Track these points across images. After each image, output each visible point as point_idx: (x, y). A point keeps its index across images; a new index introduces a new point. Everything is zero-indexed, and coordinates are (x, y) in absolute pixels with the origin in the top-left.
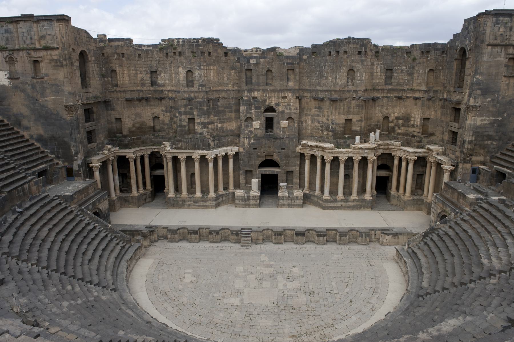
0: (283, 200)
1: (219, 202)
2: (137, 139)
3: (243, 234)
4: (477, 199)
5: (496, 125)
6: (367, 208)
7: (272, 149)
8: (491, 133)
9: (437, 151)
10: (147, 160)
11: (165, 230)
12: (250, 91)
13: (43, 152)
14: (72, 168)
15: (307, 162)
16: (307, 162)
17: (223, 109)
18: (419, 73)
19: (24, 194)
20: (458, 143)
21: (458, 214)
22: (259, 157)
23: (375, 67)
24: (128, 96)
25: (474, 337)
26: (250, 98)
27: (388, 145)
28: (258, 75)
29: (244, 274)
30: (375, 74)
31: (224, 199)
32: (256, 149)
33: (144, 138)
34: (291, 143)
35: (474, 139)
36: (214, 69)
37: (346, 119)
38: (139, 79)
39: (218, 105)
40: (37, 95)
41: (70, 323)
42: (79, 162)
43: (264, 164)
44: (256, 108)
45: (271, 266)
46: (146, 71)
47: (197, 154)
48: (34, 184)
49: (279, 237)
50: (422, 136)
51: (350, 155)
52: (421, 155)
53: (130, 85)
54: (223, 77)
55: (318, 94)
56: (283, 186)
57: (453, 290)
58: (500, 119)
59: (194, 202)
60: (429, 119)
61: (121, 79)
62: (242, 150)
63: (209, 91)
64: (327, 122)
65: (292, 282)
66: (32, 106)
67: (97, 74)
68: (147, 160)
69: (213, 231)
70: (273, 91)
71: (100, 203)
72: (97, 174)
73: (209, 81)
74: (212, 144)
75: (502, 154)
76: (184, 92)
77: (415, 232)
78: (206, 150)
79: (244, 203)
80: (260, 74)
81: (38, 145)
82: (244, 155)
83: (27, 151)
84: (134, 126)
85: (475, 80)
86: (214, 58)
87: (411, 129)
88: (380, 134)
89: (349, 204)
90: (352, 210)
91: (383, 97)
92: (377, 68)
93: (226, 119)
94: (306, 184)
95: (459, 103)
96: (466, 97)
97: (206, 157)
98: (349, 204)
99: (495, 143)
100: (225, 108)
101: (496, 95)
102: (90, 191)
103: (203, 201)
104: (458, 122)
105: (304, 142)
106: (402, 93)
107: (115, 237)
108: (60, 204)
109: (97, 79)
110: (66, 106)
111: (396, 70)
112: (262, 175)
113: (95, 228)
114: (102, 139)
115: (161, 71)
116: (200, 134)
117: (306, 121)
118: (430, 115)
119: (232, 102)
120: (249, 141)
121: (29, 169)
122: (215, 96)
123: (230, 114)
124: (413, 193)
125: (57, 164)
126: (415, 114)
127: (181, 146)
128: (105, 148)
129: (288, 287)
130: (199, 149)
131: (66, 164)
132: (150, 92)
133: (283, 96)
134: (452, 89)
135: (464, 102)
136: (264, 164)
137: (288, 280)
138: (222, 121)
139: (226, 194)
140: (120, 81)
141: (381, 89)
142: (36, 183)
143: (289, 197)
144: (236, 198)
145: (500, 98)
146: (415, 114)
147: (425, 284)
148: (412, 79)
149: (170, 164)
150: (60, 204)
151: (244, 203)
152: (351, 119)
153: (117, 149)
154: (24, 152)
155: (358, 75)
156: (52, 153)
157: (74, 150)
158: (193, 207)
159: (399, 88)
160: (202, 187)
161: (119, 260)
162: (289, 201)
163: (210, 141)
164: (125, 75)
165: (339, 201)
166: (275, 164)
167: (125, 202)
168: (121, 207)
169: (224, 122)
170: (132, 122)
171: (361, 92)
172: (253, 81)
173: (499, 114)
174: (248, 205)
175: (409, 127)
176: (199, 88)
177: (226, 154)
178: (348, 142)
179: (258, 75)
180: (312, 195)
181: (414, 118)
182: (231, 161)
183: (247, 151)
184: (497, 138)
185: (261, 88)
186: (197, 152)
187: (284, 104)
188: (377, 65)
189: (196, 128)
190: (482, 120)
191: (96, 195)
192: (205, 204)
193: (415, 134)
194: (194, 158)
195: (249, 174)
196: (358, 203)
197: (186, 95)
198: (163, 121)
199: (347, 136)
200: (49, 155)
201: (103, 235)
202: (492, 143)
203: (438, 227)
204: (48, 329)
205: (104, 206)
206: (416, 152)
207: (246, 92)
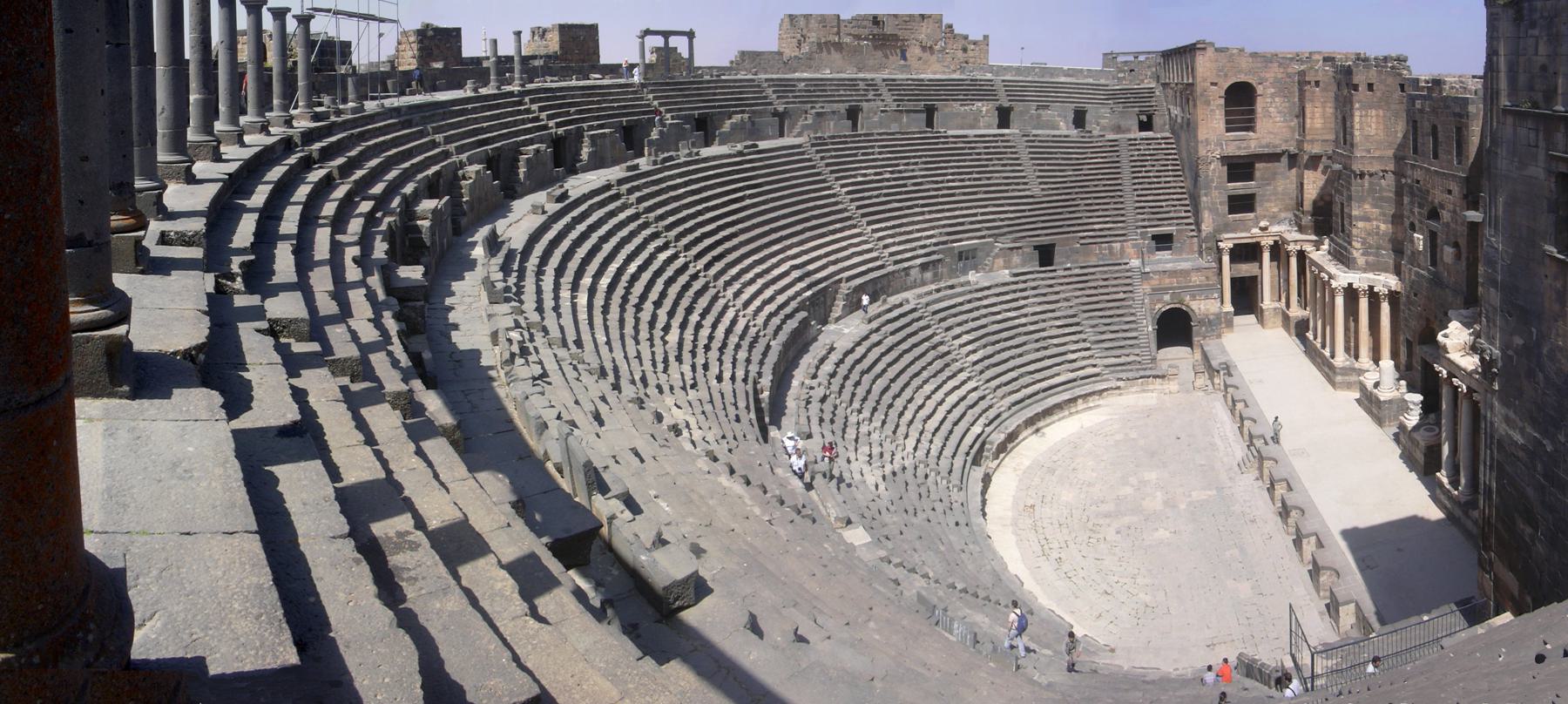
71: (1193, 298)
72: (1226, 259)
73: (1367, 137)
74: (1361, 261)
86: (1378, 94)
122: (1375, 167)
163: (1356, 254)
177: (1371, 288)
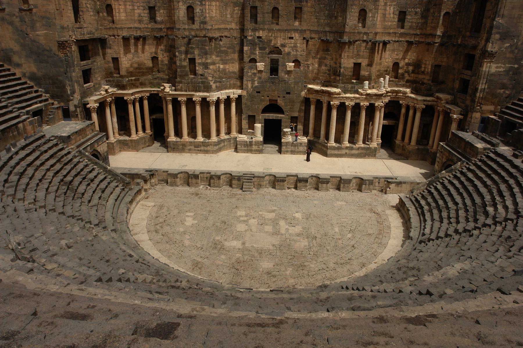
0: (286, 146)
1: (219, 147)
2: (135, 80)
3: (245, 179)
4: (485, 149)
5: (511, 73)
6: (372, 156)
7: (276, 92)
8: (505, 80)
9: (446, 100)
10: (146, 103)
11: (165, 174)
12: (254, 30)
13: (36, 91)
14: (68, 109)
15: (313, 108)
16: (313, 108)
17: (225, 49)
18: (433, 16)
19: (19, 133)
20: (470, 91)
21: (465, 164)
22: (262, 101)
23: (388, 8)
24: (125, 34)
25: (485, 280)
26: (254, 38)
27: (397, 92)
28: (263, 13)
29: (246, 219)
30: (387, 16)
31: (226, 143)
32: (259, 92)
33: (142, 79)
34: (296, 87)
35: (486, 87)
36: (216, 5)
37: (355, 64)
38: (136, 15)
39: (220, 45)
40: (26, 29)
41: (68, 260)
42: (76, 102)
43: (266, 110)
44: (261, 49)
45: (273, 211)
46: (144, 7)
47: (198, 96)
48: (28, 124)
49: (282, 183)
50: (432, 84)
51: (358, 101)
52: (430, 103)
53: (127, 22)
54: (226, 14)
55: (326, 36)
56: (287, 132)
57: (457, 237)
58: (516, 66)
59: (195, 147)
60: (440, 66)
61: (117, 14)
62: (244, 93)
63: (211, 29)
64: (334, 65)
65: (295, 227)
66: (22, 41)
67: (91, 9)
68: (146, 103)
69: (214, 175)
70: (279, 30)
72: (94, 116)
73: (211, 17)
74: (214, 86)
75: (513, 104)
76: (184, 29)
77: (418, 181)
78: (207, 91)
79: (246, 148)
80: (265, 11)
81: (32, 84)
82: (247, 100)
83: (20, 90)
84: (131, 66)
85: (495, 23)
87: (421, 77)
88: (389, 81)
89: (354, 152)
90: (356, 158)
91: (395, 41)
92: (390, 9)
93: (228, 60)
94: (311, 131)
95: (475, 47)
96: (483, 42)
97: (208, 99)
98: (354, 152)
99: (507, 92)
100: (228, 48)
101: (515, 40)
102: (88, 133)
103: (204, 146)
104: (471, 70)
105: (310, 86)
106: (414, 38)
107: (115, 179)
108: (56, 145)
109: (92, 13)
110: (58, 42)
111: (410, 12)
112: (265, 120)
113: (93, 169)
114: (99, 79)
115: (159, 7)
116: (202, 75)
117: (313, 64)
118: (442, 62)
119: (236, 42)
120: (253, 83)
121: (23, 108)
122: (217, 35)
123: (233, 55)
124: (418, 142)
125: (53, 104)
126: (426, 61)
127: (182, 88)
128: (102, 89)
129: (290, 232)
130: (200, 91)
131: (62, 104)
132: (148, 30)
133: (289, 36)
134: (468, 34)
135: (480, 47)
136: (266, 110)
137: (290, 225)
138: (225, 62)
139: (228, 139)
140: (116, 16)
141: (393, 33)
142: (31, 123)
143: (293, 143)
144: (238, 143)
145: (519, 43)
146: (426, 61)
147: (427, 231)
148: (426, 23)
149: (170, 107)
150: (56, 145)
151: (246, 148)
152: (360, 64)
153: (115, 89)
154: (17, 91)
155: (370, 15)
156: (46, 92)
157: (70, 90)
158: (194, 152)
159: (412, 32)
160: (203, 131)
161: (118, 202)
162: (293, 148)
163: (212, 83)
164: (122, 10)
165: (343, 149)
166: (280, 110)
167: (125, 146)
168: (120, 151)
169: (226, 64)
170: (130, 62)
171: (372, 34)
172: (258, 19)
173: (517, 60)
174: (251, 151)
175: (418, 73)
176: (200, 26)
177: (228, 97)
178: (356, 87)
179: (263, 13)
180: (316, 142)
181: (425, 64)
182: (233, 105)
183: (250, 95)
184: (510, 86)
185: (266, 27)
186: (197, 94)
187: (290, 45)
188: (390, 5)
189: (197, 68)
190: (497, 67)
191: (94, 137)
192: (206, 148)
193: (425, 81)
194: (195, 101)
195: (252, 120)
196: (362, 151)
197: (187, 33)
198: (162, 61)
199: (355, 81)
200: (44, 95)
201: (101, 177)
202: (504, 92)
203: (443, 176)
204: (45, 265)
205: (102, 148)
206: (424, 101)
207: (250, 31)
